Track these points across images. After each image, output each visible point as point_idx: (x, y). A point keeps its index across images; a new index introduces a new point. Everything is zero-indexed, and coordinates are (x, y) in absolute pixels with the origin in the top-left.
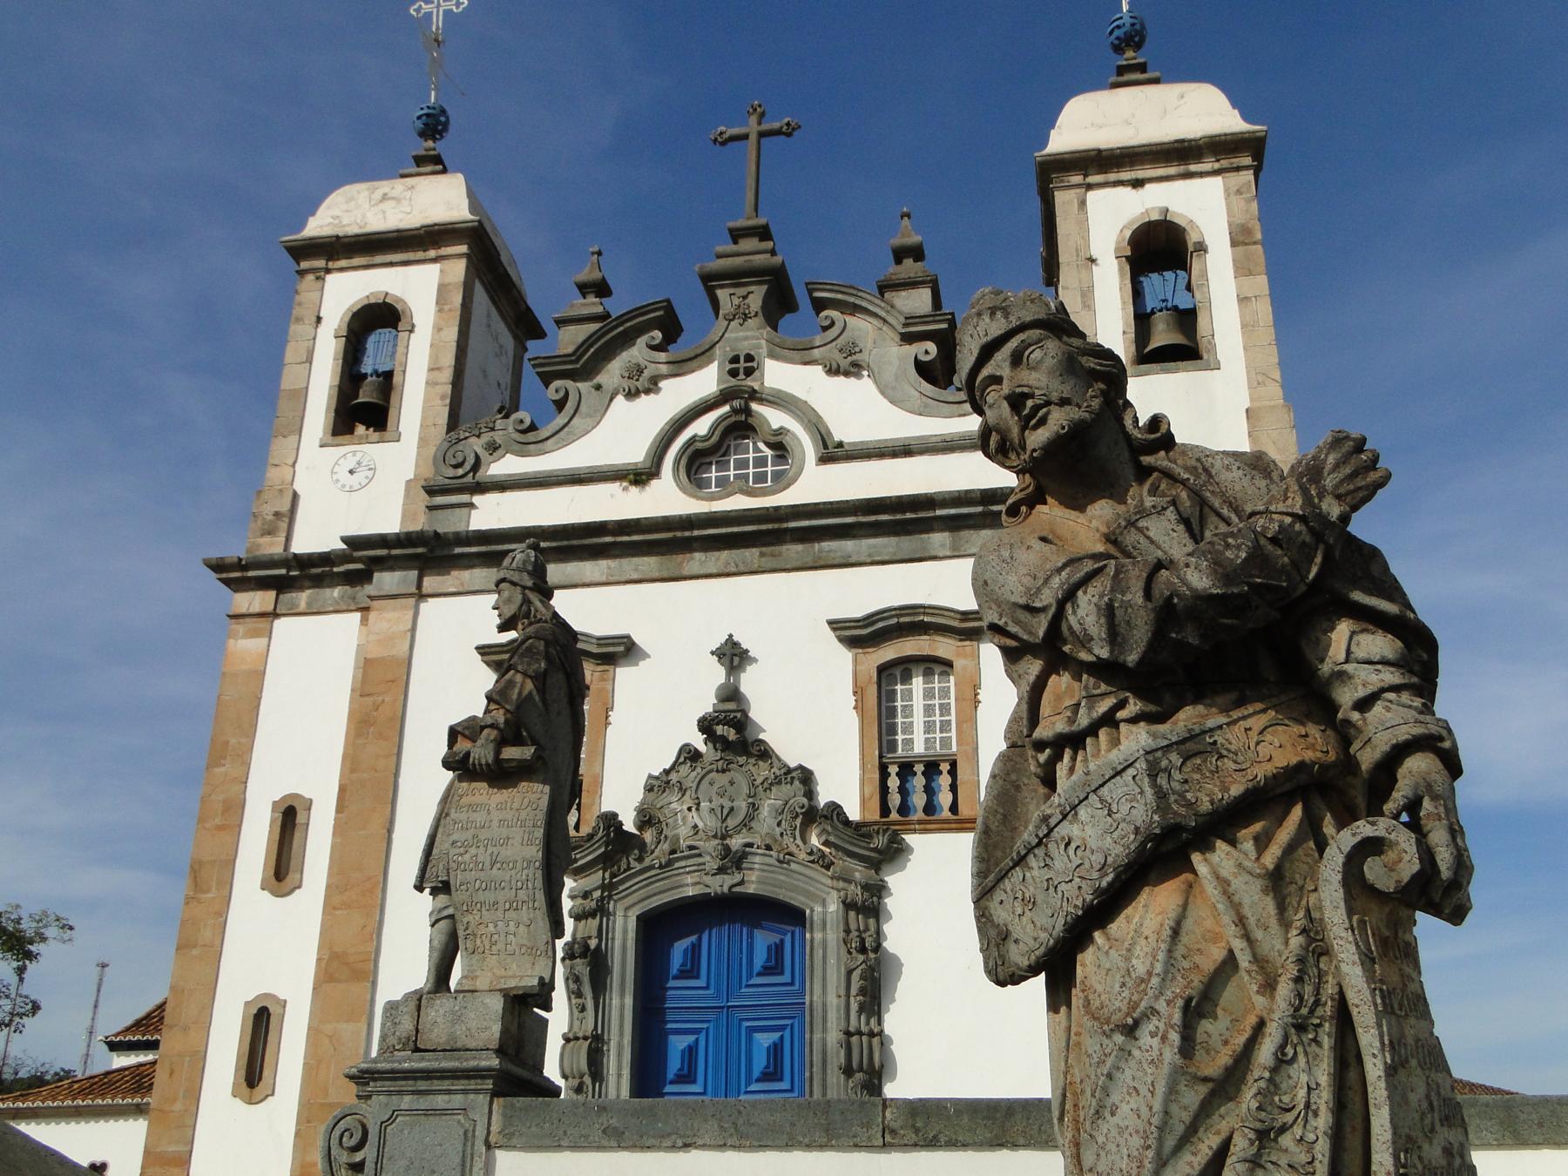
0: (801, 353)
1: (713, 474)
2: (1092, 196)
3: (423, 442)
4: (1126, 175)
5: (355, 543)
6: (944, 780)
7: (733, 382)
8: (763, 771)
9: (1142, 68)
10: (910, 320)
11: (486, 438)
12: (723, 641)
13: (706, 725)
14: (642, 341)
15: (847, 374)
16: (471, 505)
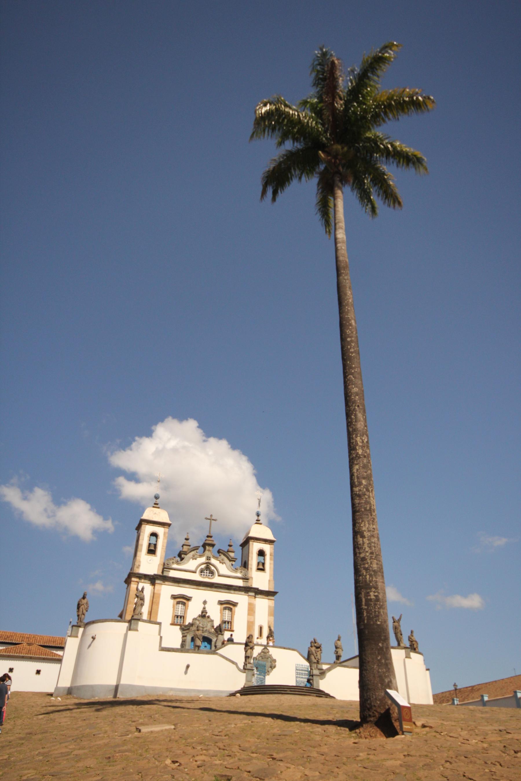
0: (216, 558)
1: (203, 574)
2: (254, 543)
3: (161, 558)
4: (259, 542)
5: (155, 575)
6: (230, 624)
7: (207, 561)
8: (209, 620)
9: (259, 520)
10: (232, 558)
11: (172, 561)
12: (204, 600)
13: (202, 612)
14: (195, 551)
15: (223, 563)
16: (169, 571)
